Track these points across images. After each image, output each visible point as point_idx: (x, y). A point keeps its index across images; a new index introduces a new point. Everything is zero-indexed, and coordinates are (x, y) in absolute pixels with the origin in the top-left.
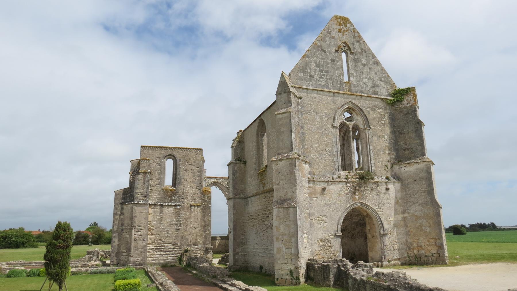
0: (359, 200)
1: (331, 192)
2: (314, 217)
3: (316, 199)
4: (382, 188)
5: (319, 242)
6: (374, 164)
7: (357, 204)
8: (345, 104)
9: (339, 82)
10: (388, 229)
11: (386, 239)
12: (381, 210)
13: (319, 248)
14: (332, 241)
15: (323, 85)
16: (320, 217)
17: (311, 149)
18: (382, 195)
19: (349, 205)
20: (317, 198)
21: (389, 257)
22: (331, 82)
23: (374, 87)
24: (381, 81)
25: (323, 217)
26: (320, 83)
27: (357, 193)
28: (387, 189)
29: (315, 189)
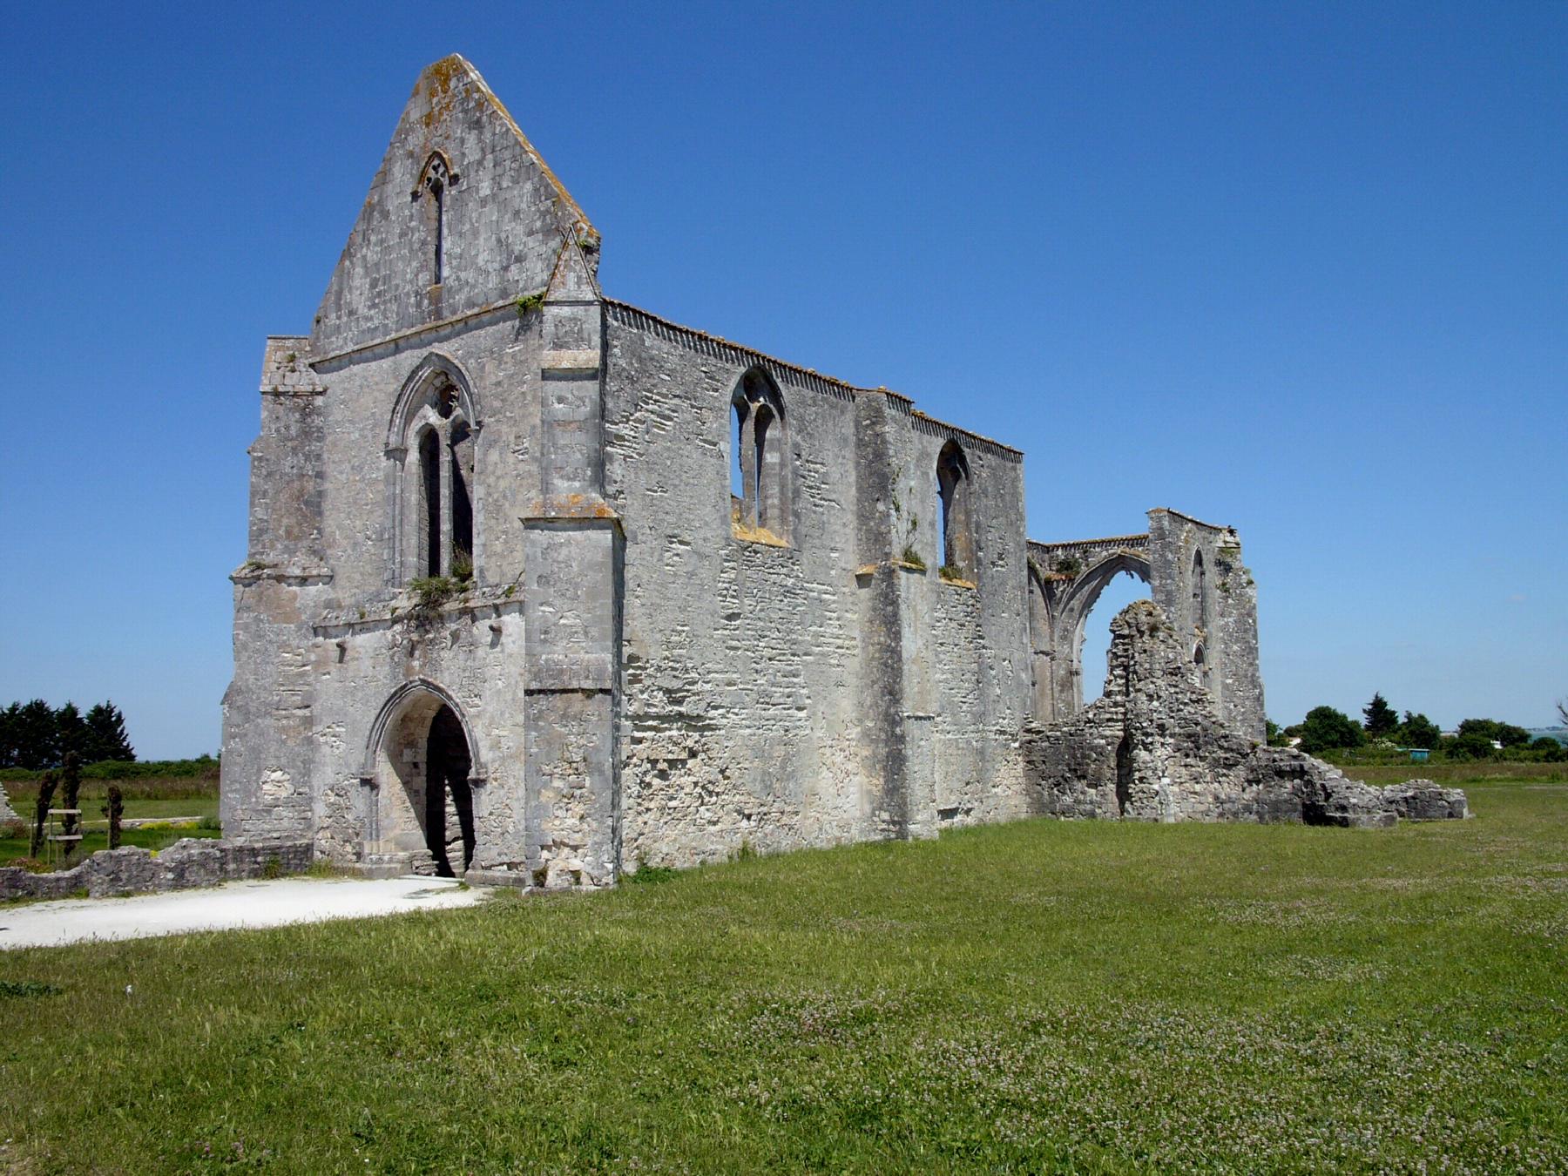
0: (420, 672)
1: (357, 656)
2: (320, 728)
3: (328, 676)
4: (482, 629)
5: (327, 795)
6: (484, 545)
7: (413, 684)
8: (419, 367)
9: (413, 300)
10: (489, 765)
11: (483, 797)
12: (476, 700)
13: (328, 812)
14: (352, 793)
15: (377, 328)
16: (334, 726)
17: (337, 533)
18: (480, 652)
19: (393, 690)
20: (329, 673)
21: (485, 855)
22: (395, 307)
23: (506, 269)
24: (531, 233)
25: (338, 726)
26: (369, 324)
27: (417, 653)
28: (496, 631)
29: (326, 650)
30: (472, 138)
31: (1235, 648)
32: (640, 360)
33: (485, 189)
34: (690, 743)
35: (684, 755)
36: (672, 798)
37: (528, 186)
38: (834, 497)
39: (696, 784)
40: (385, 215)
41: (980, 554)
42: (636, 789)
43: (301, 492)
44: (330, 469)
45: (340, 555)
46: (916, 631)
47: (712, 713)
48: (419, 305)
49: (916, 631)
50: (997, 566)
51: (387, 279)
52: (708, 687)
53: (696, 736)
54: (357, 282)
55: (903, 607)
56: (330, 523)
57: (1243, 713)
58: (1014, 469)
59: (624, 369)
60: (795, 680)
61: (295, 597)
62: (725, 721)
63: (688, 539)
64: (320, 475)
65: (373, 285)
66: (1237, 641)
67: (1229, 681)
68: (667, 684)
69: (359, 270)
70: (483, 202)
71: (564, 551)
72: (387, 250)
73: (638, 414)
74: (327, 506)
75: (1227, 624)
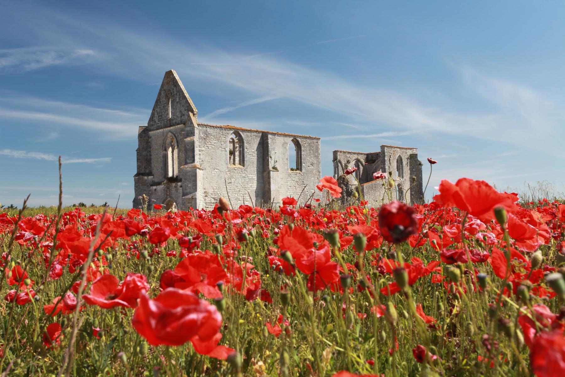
23: (181, 117)
24: (185, 110)
30: (175, 88)
32: (206, 134)
33: (178, 100)
37: (185, 101)
40: (160, 102)
43: (147, 159)
44: (152, 154)
45: (154, 171)
48: (167, 122)
51: (161, 116)
54: (156, 116)
55: (271, 180)
56: (153, 165)
58: (317, 142)
61: (146, 180)
64: (151, 155)
65: (159, 117)
68: (213, 197)
69: (156, 113)
70: (177, 102)
71: (189, 174)
72: (161, 110)
74: (152, 161)
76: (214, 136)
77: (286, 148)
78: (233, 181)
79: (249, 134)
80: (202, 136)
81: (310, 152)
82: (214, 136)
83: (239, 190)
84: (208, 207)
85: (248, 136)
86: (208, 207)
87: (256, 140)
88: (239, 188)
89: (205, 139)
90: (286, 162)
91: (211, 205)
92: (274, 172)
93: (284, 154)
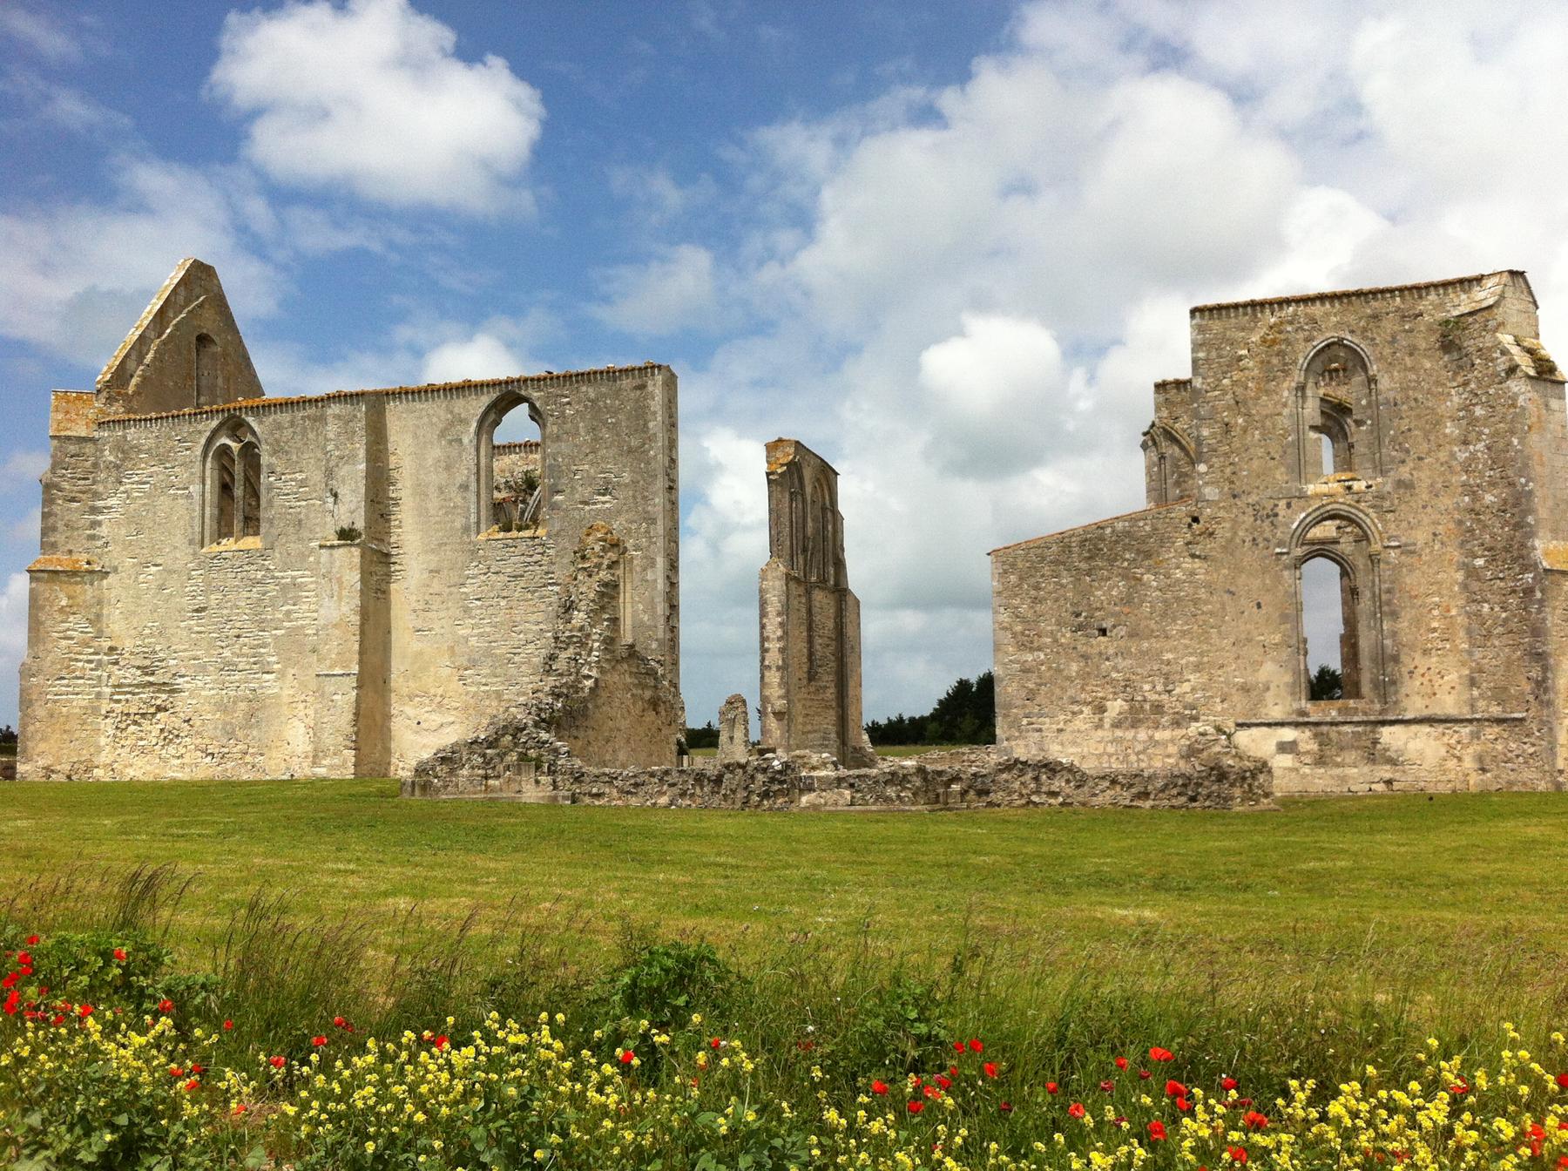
31: (1489, 498)
32: (123, 452)
34: (159, 702)
35: (152, 710)
36: (142, 739)
38: (314, 495)
39: (162, 730)
41: (559, 498)
42: (111, 732)
46: (340, 599)
47: (180, 680)
49: (340, 599)
50: (595, 504)
52: (172, 662)
53: (164, 696)
57: (1506, 620)
58: (642, 387)
59: (111, 462)
60: (262, 650)
62: (189, 686)
63: (159, 562)
66: (1493, 484)
67: (1480, 562)
68: (138, 663)
73: (122, 489)
75: (1473, 458)
76: (148, 451)
77: (460, 441)
78: (213, 603)
79: (284, 417)
80: (112, 458)
81: (595, 439)
82: (148, 451)
83: (236, 632)
84: (118, 701)
85: (279, 427)
86: (118, 701)
87: (311, 436)
88: (238, 624)
89: (117, 467)
90: (459, 501)
91: (130, 693)
92: (341, 550)
93: (448, 468)
